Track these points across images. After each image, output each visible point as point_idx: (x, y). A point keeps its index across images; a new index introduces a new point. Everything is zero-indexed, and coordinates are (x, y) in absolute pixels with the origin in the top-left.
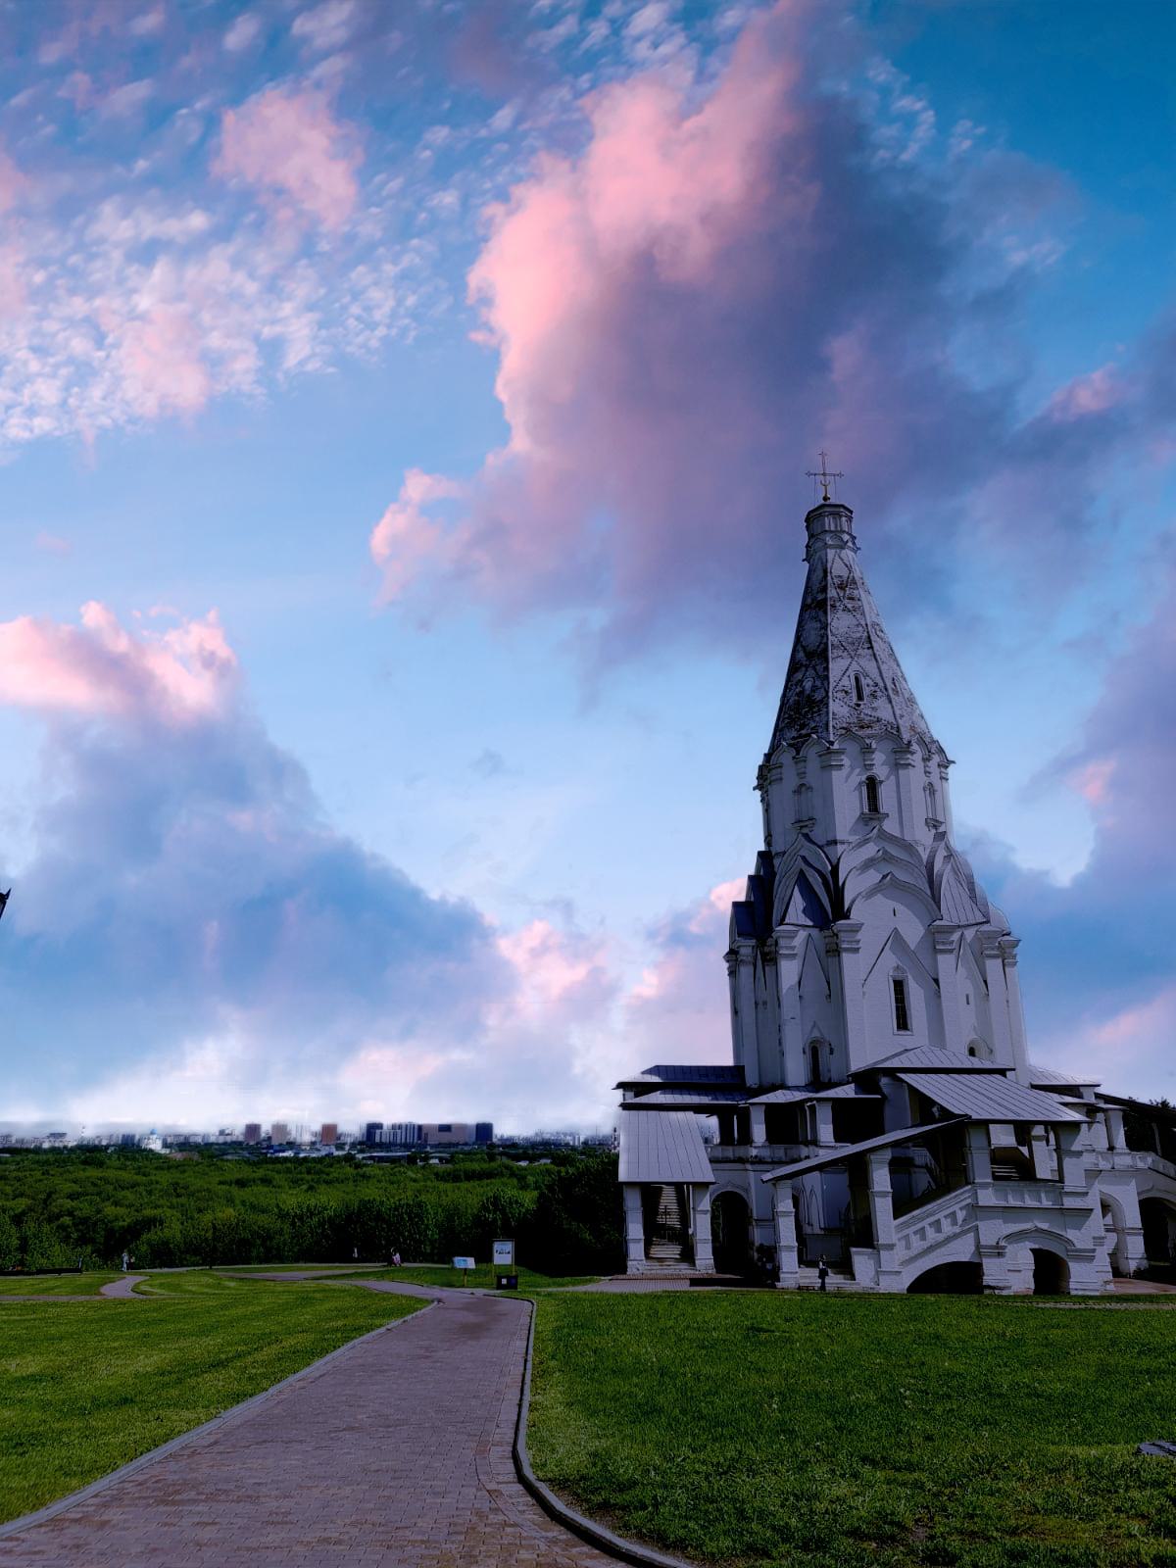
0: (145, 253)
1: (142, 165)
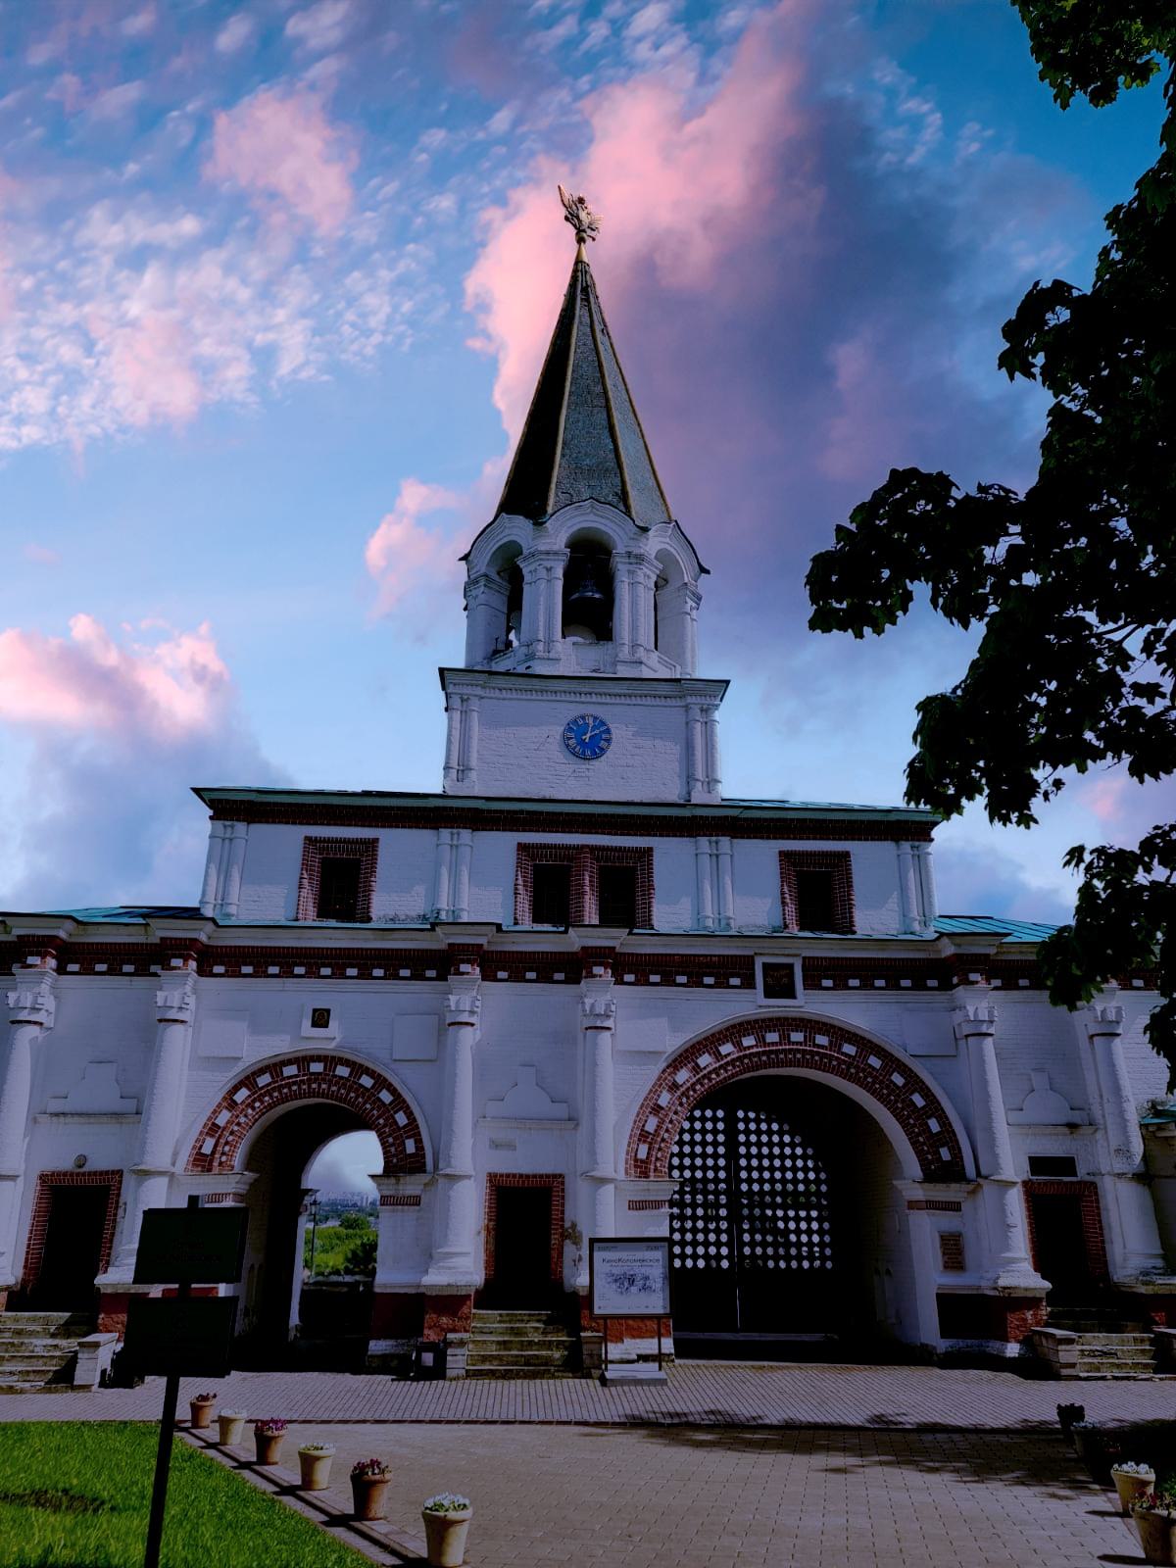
0: (136, 259)
1: (132, 168)
